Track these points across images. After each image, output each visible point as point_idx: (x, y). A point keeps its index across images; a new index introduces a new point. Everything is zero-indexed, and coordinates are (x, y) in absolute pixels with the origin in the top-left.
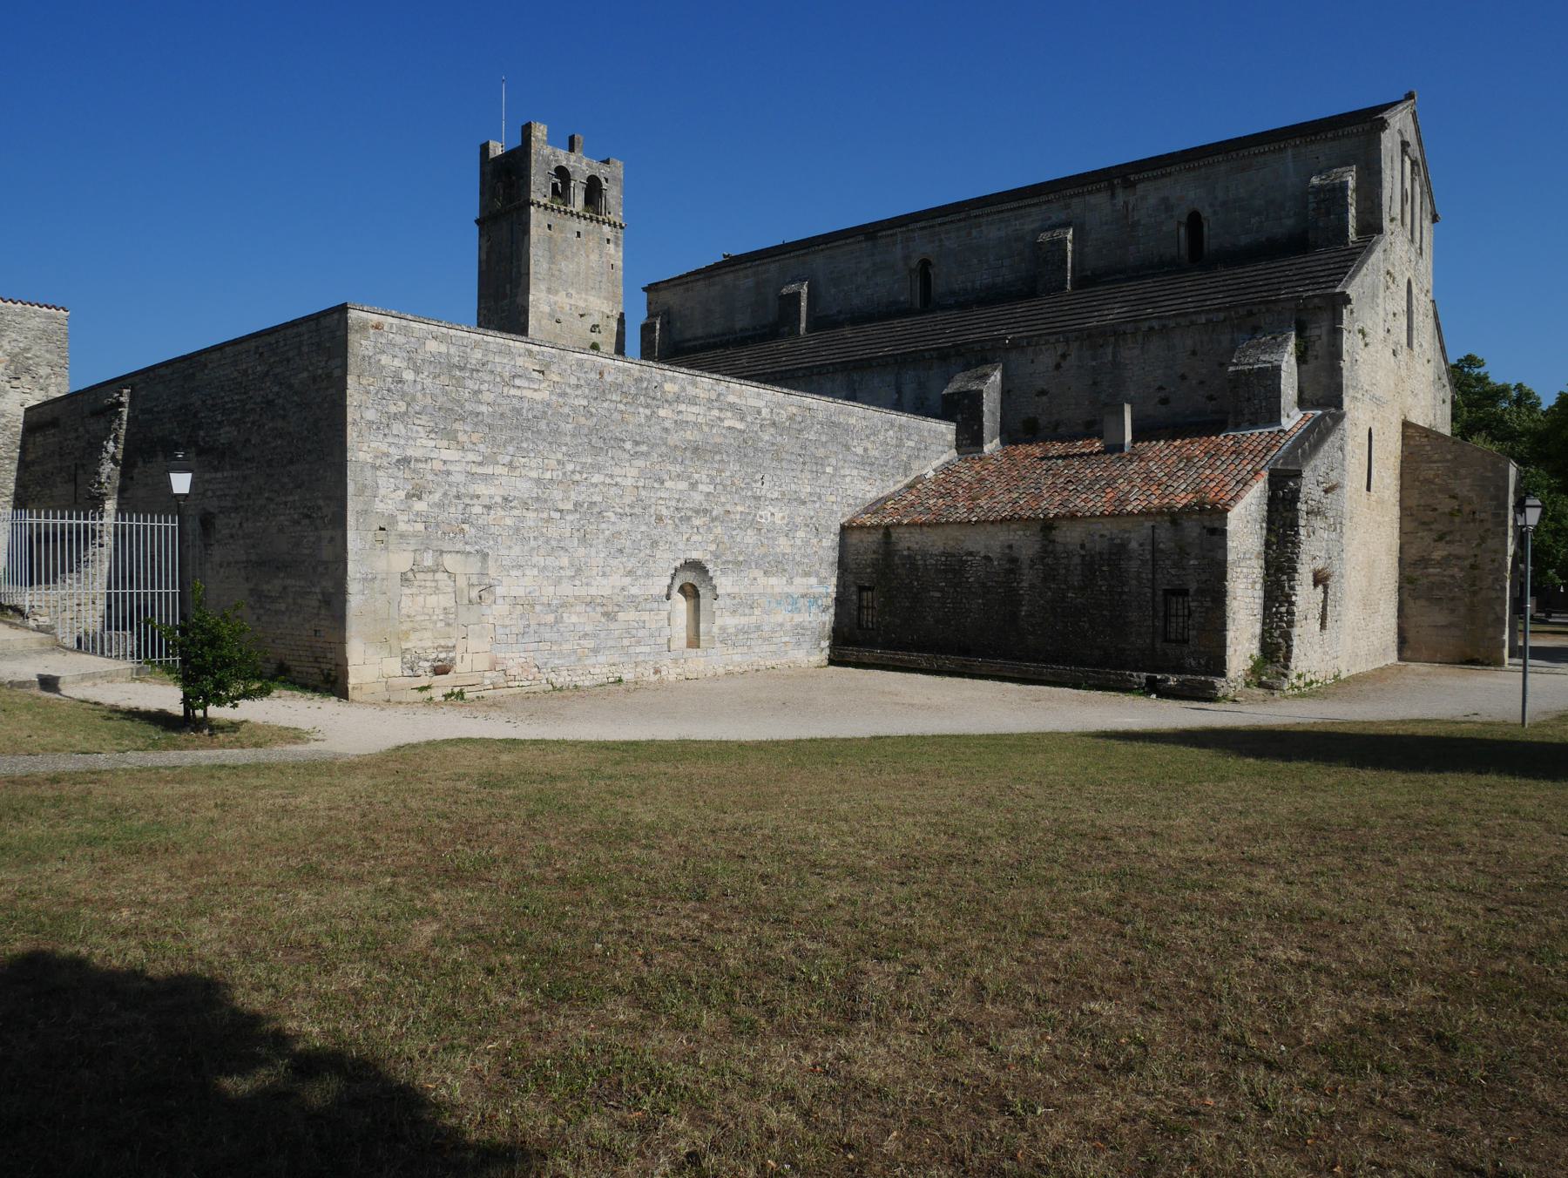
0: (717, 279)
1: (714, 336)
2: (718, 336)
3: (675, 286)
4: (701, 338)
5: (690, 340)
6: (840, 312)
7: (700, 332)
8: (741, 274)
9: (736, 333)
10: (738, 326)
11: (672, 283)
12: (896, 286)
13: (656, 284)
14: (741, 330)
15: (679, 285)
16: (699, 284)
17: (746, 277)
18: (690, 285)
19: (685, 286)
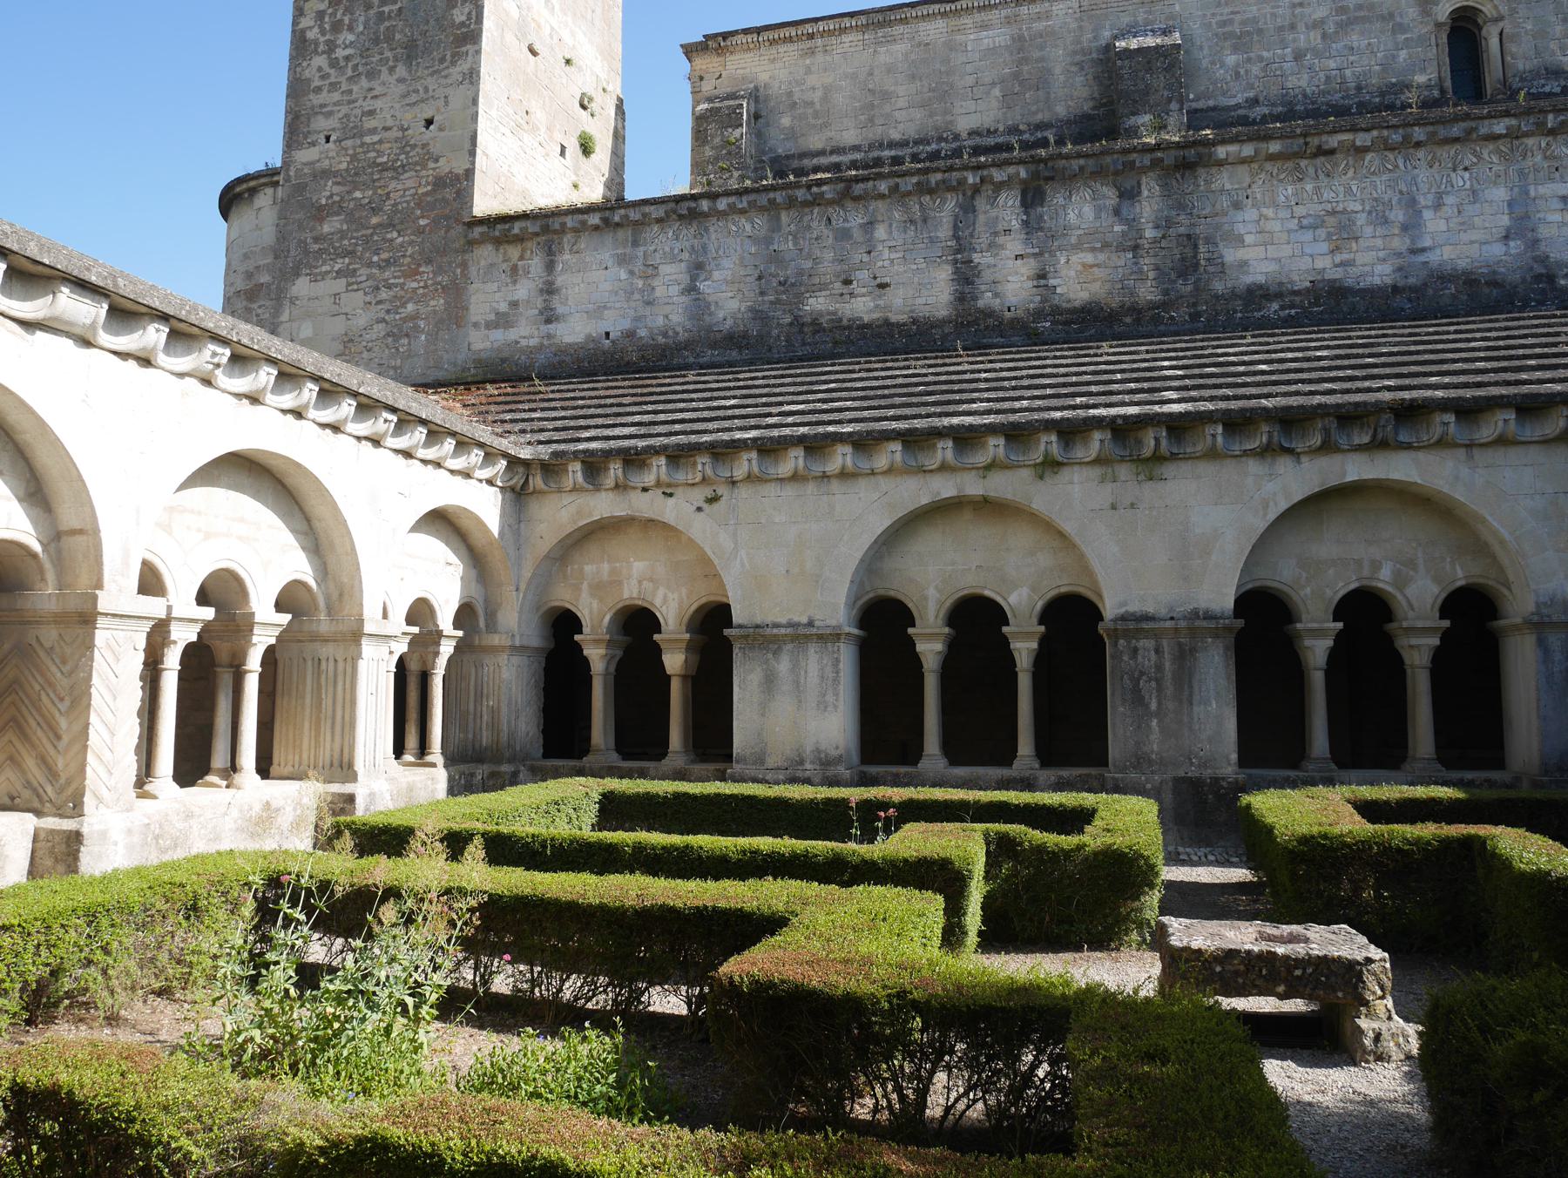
0: (898, 30)
1: (892, 145)
2: (904, 144)
3: (773, 42)
4: (856, 148)
5: (822, 153)
6: (1255, 102)
7: (850, 136)
8: (967, 21)
9: (956, 137)
10: (964, 125)
11: (765, 36)
12: (1403, 54)
13: (726, 36)
14: (973, 133)
15: (790, 40)
16: (846, 38)
17: (984, 27)
18: (819, 42)
19: (809, 44)
